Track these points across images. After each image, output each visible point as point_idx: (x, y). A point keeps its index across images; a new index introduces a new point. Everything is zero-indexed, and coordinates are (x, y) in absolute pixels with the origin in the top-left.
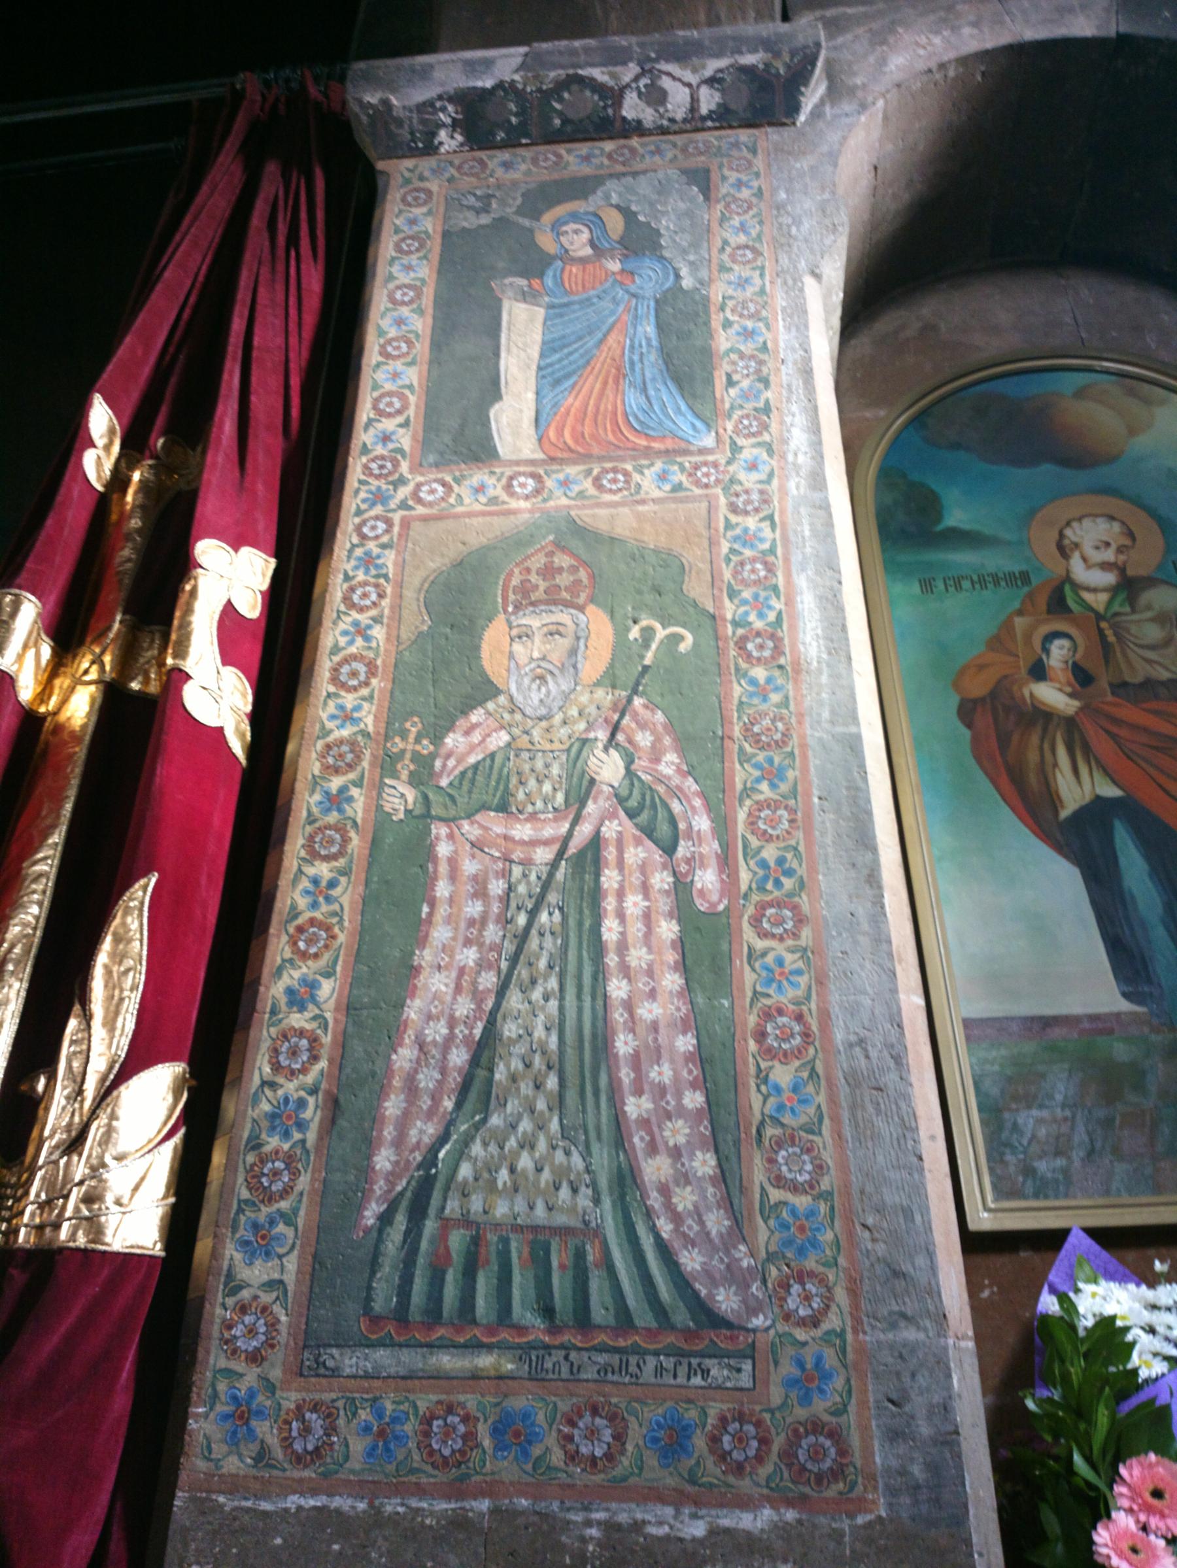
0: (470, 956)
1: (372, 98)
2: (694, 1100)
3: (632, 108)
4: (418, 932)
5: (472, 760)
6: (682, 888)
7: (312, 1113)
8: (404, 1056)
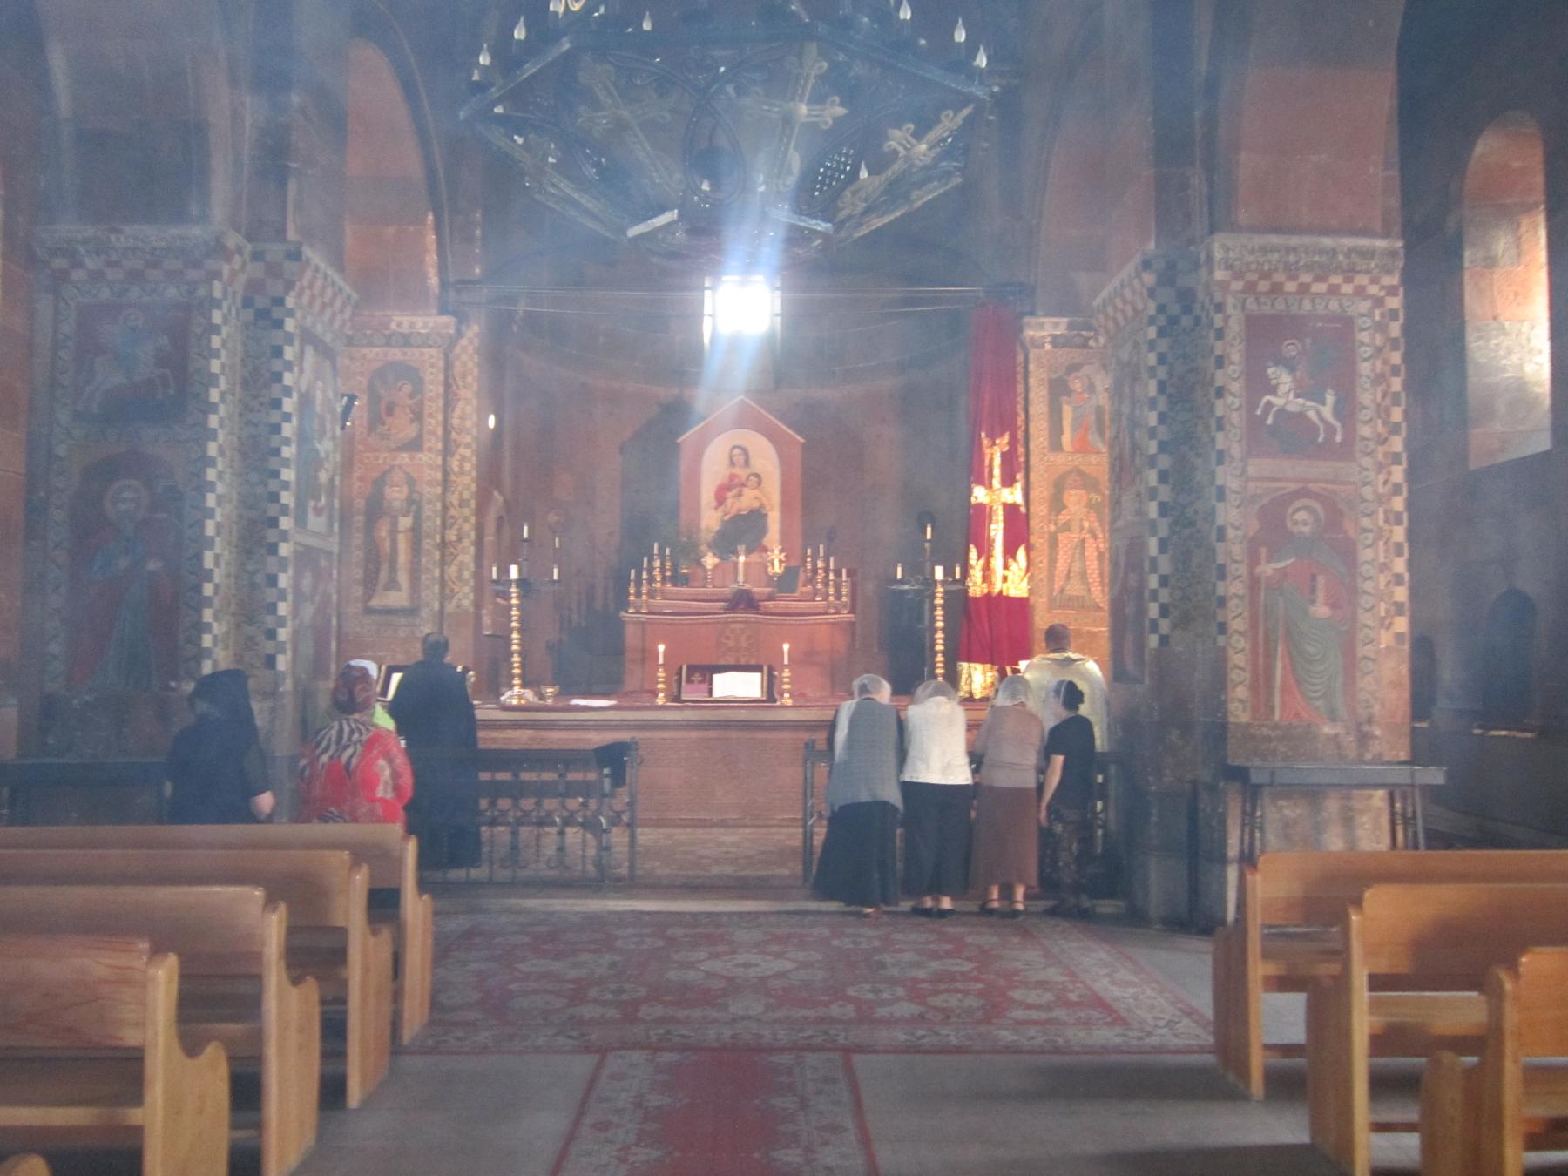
0: (1065, 557)
1: (1031, 333)
2: (1098, 580)
3: (1091, 343)
4: (1057, 554)
5: (1064, 521)
6: (1098, 547)
7: (1045, 579)
8: (1057, 572)
